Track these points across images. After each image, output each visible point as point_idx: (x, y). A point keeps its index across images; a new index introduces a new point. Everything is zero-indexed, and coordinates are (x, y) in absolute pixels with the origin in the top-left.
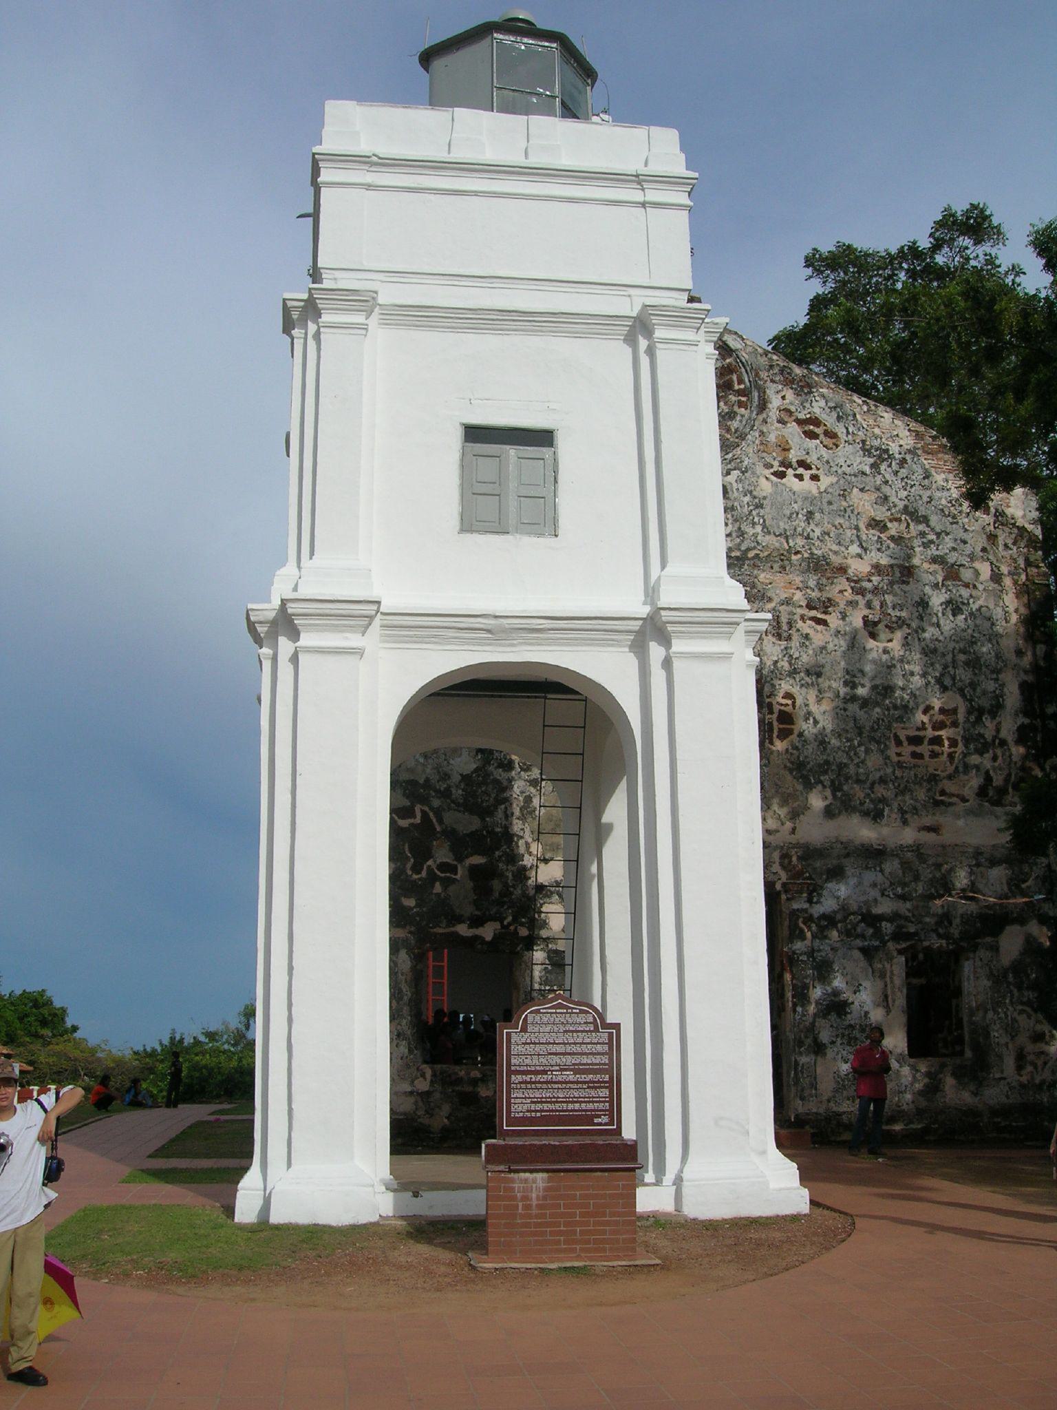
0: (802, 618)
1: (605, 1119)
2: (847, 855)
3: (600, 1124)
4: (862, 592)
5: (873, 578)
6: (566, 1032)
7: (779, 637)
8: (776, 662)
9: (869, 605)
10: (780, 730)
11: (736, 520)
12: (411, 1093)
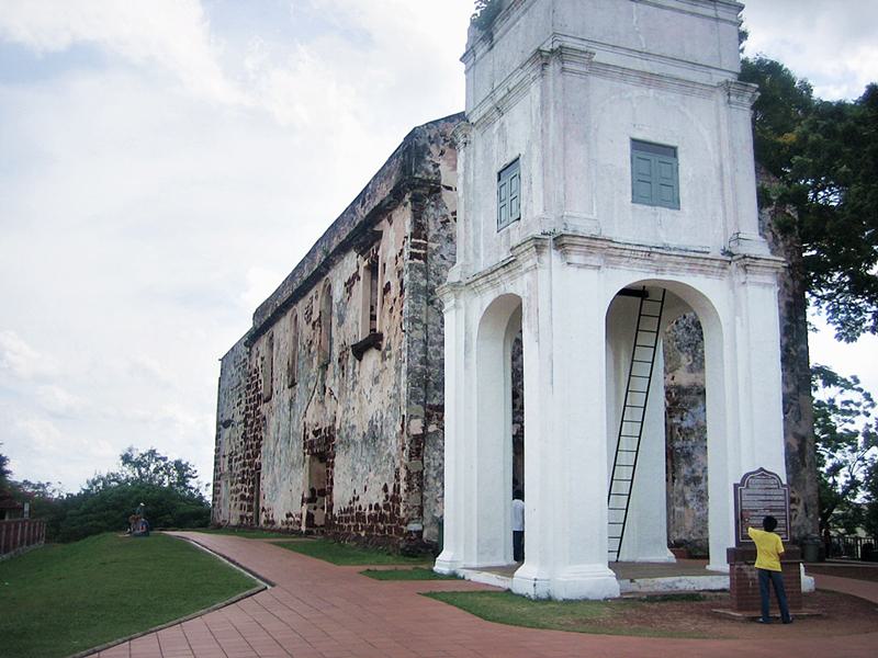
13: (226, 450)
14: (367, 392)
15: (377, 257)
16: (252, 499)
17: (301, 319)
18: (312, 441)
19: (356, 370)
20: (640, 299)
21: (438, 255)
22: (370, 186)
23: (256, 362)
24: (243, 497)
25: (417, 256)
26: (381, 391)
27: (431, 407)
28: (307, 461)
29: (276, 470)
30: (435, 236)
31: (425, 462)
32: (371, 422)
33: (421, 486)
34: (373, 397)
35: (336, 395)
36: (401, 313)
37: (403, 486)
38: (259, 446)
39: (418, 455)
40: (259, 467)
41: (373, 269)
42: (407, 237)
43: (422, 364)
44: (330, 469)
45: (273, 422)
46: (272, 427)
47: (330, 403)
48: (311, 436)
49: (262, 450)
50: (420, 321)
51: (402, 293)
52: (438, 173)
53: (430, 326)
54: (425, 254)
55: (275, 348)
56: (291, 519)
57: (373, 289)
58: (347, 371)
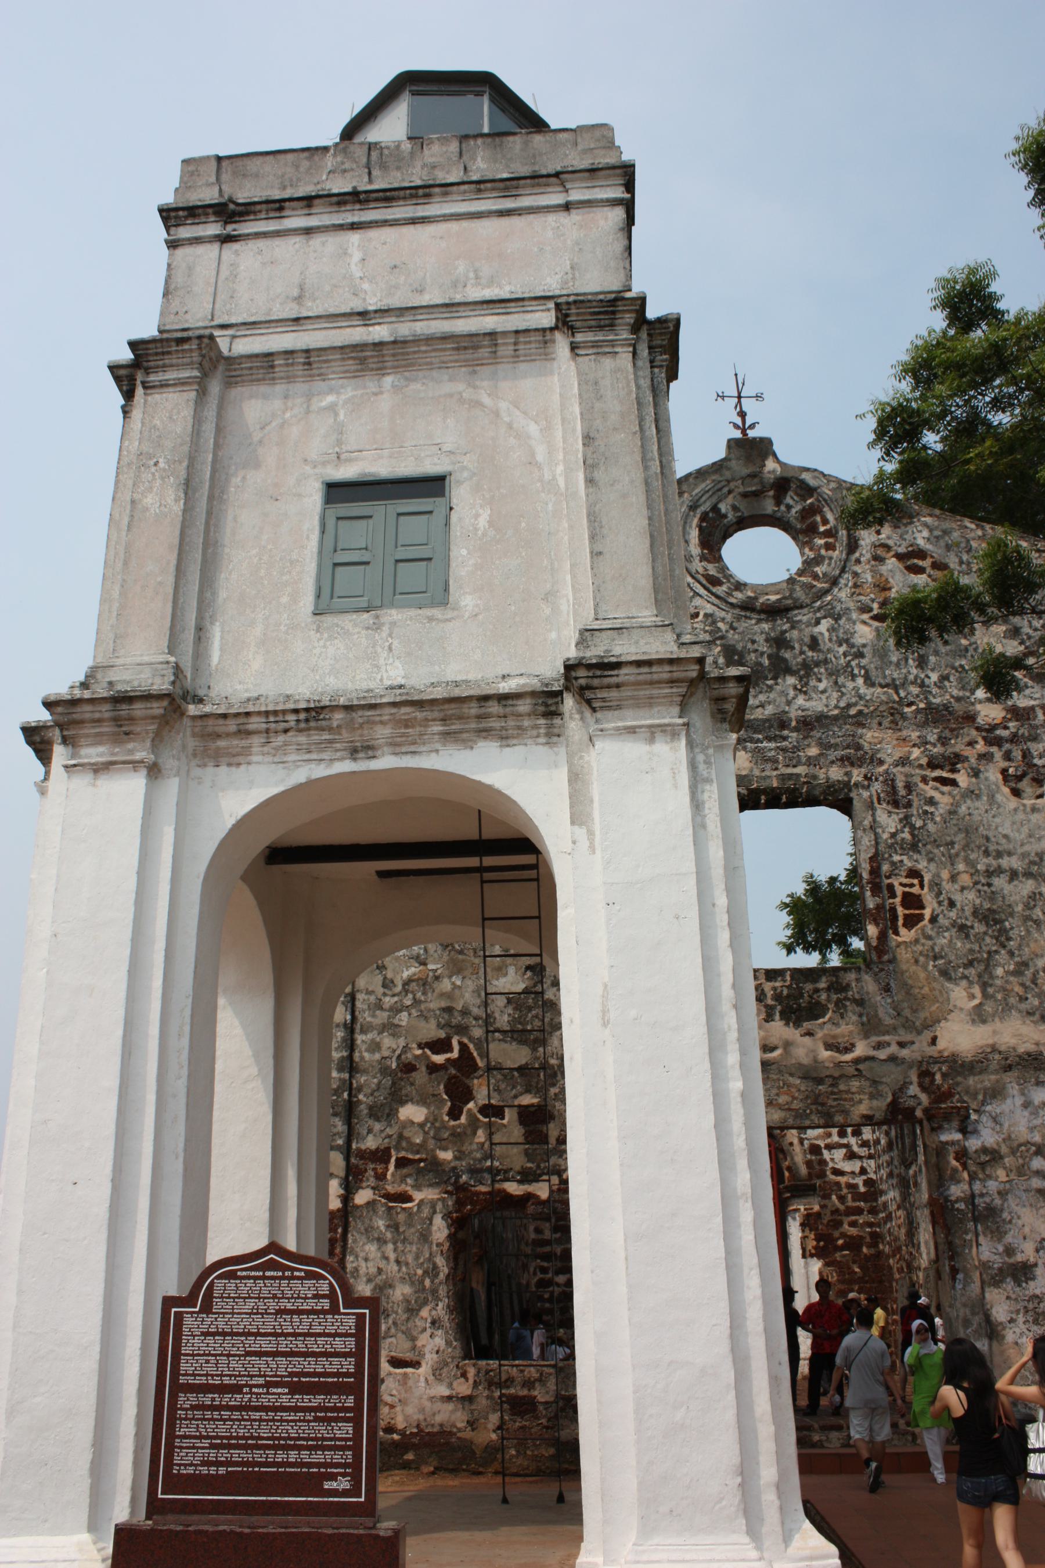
0: (925, 780)
1: (344, 1484)
2: (1009, 1068)
3: (334, 1493)
4: (998, 742)
5: (1011, 724)
6: (280, 1312)
7: (896, 804)
8: (893, 835)
9: (1007, 757)
10: (906, 916)
11: (830, 674)
12: (449, 1398)
27: (362, 1154)
53: (360, 997)
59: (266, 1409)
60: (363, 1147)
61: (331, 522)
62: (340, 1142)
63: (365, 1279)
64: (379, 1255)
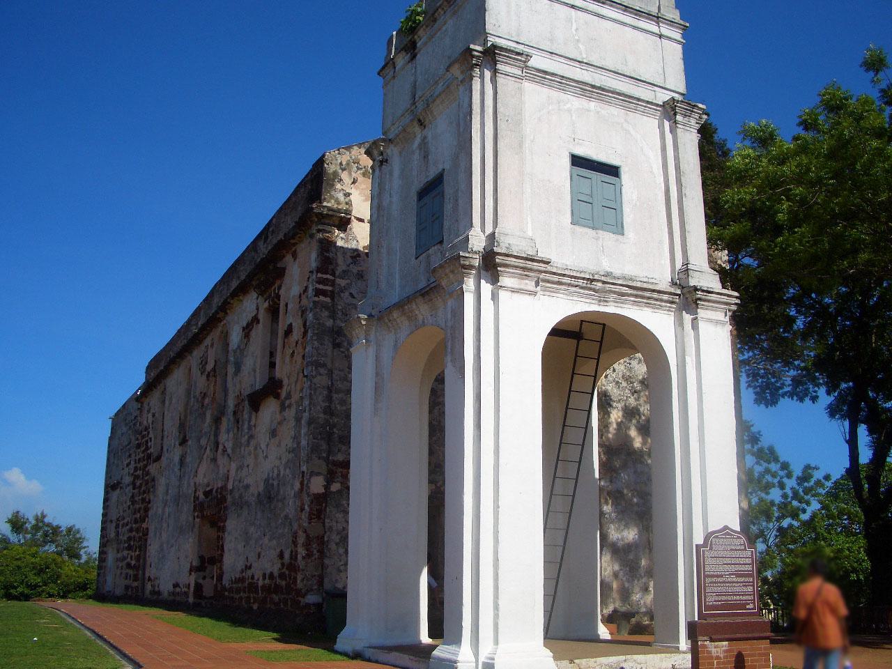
1: (751, 606)
6: (732, 550)
13: (114, 515)
14: (263, 446)
15: (278, 297)
16: (138, 568)
17: (196, 371)
18: (202, 504)
19: (252, 423)
20: (576, 341)
21: (347, 294)
22: (274, 220)
23: (147, 419)
24: (129, 565)
25: (323, 293)
26: (279, 445)
28: (197, 526)
29: (164, 536)
30: (344, 271)
31: (327, 524)
32: (267, 481)
33: (321, 552)
34: (269, 451)
35: (229, 451)
36: (304, 356)
37: (302, 551)
38: (147, 510)
39: (319, 517)
40: (146, 533)
41: (274, 312)
42: (311, 272)
43: (325, 413)
44: (221, 534)
45: (162, 482)
46: (161, 489)
47: (222, 460)
48: (202, 497)
49: (150, 513)
50: (324, 365)
51: (305, 333)
52: (349, 203)
53: (336, 372)
54: (332, 292)
55: (167, 402)
56: (178, 590)
57: (274, 333)
58: (242, 425)
59: (730, 583)
60: (336, 459)
61: (575, 176)
62: (325, 455)
63: (336, 533)
64: (343, 520)
